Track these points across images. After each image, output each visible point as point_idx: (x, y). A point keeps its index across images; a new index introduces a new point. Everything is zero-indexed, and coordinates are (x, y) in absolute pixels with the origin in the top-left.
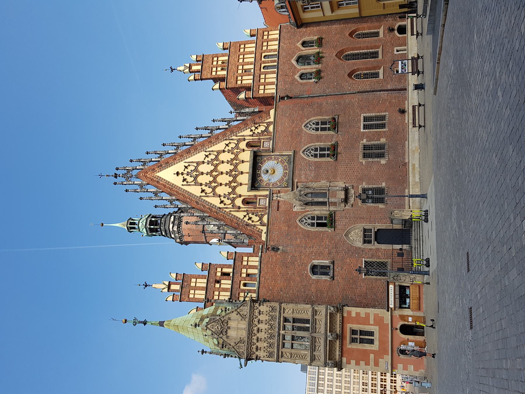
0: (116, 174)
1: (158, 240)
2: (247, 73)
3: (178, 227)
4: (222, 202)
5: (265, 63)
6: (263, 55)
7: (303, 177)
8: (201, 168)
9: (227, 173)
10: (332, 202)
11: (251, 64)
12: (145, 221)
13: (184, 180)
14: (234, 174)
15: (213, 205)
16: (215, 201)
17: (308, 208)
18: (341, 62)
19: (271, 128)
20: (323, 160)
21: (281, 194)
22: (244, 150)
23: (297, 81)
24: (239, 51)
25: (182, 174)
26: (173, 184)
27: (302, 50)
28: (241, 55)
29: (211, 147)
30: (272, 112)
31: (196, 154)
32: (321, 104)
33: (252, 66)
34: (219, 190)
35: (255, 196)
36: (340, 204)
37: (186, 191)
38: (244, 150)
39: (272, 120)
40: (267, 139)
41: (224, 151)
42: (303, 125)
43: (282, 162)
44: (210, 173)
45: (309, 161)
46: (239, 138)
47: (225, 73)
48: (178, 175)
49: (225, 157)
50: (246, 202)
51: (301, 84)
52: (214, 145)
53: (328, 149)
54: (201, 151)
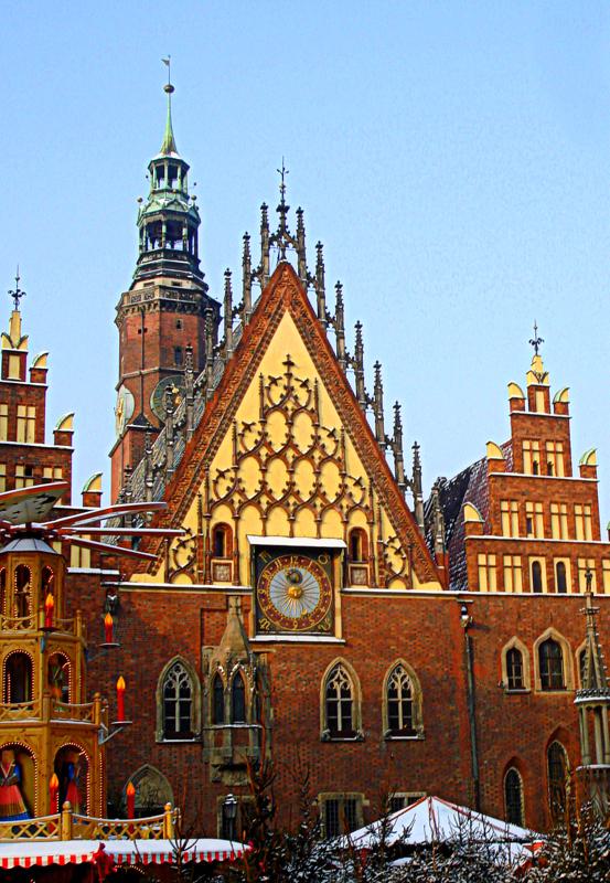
0: (288, 208)
1: (133, 242)
2: (525, 525)
3: (163, 303)
4: (222, 474)
5: (547, 566)
6: (567, 562)
7: (282, 666)
8: (303, 421)
9: (291, 484)
10: (221, 734)
11: (548, 533)
12: (179, 209)
13: (274, 381)
14: (290, 501)
15: (214, 454)
16: (223, 459)
17: (207, 681)
18: (546, 741)
19: (398, 587)
20: (321, 708)
21: (241, 617)
22: (346, 523)
23: (506, 641)
24: (575, 504)
25: (289, 375)
26: (263, 353)
27: (574, 652)
28: (568, 508)
29: (354, 444)
30: (434, 588)
31: (337, 408)
32: (450, 701)
33: (541, 537)
34: (250, 465)
35: (238, 556)
36: (219, 753)
37: (247, 386)
38: (346, 523)
39: (420, 588)
40: (373, 579)
41: (343, 476)
42: (403, 662)
43: (317, 614)
44: (290, 443)
45: (319, 679)
46: (376, 512)
47: (528, 473)
48: (285, 363)
49: (331, 479)
50: (221, 529)
51: (498, 653)
52: (357, 450)
53: (346, 723)
54: (343, 420)
